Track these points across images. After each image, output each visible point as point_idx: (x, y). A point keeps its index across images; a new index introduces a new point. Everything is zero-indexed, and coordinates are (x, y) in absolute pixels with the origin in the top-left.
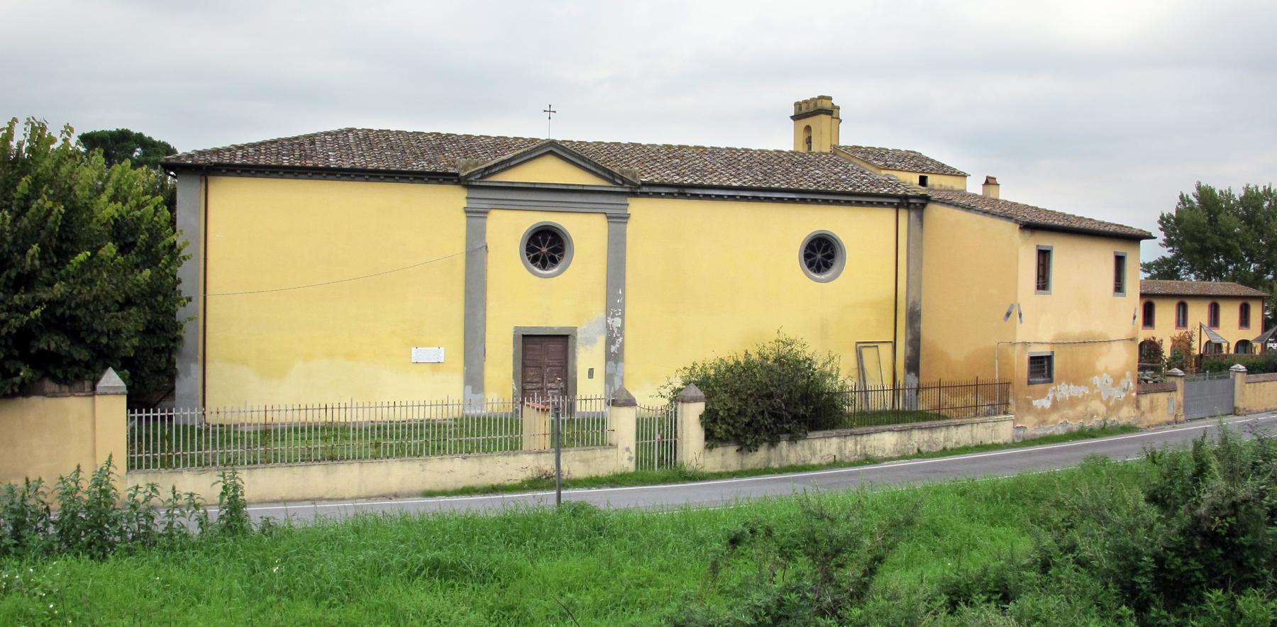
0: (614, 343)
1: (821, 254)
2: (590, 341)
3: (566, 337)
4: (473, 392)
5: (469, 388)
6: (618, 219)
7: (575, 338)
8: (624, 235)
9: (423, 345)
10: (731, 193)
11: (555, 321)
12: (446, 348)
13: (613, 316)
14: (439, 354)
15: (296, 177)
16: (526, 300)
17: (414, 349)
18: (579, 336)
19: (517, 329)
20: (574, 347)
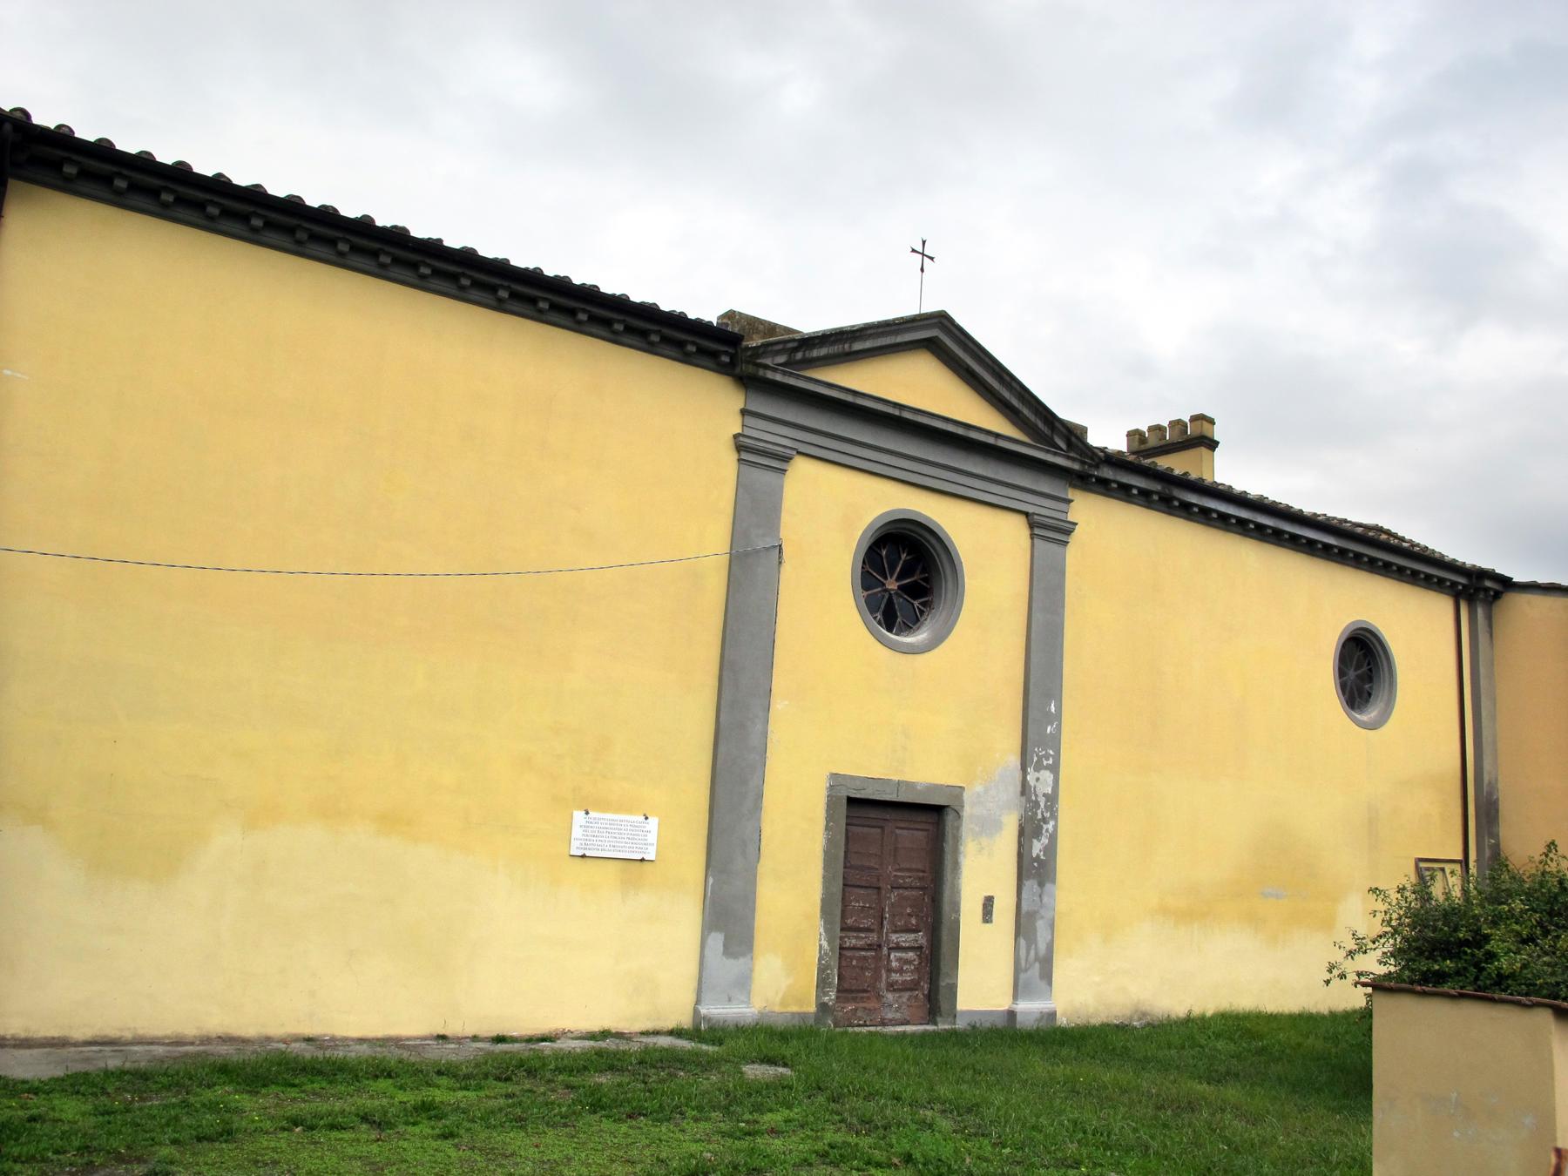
0: (1037, 833)
1: (1363, 666)
2: (990, 826)
3: (937, 811)
4: (729, 951)
5: (717, 940)
6: (1051, 532)
7: (958, 816)
8: (1062, 573)
9: (604, 806)
10: (1244, 514)
11: (919, 768)
12: (661, 824)
13: (1039, 767)
14: (647, 838)
15: (340, 261)
16: (870, 710)
17: (579, 816)
18: (967, 811)
19: (836, 780)
20: (957, 839)
